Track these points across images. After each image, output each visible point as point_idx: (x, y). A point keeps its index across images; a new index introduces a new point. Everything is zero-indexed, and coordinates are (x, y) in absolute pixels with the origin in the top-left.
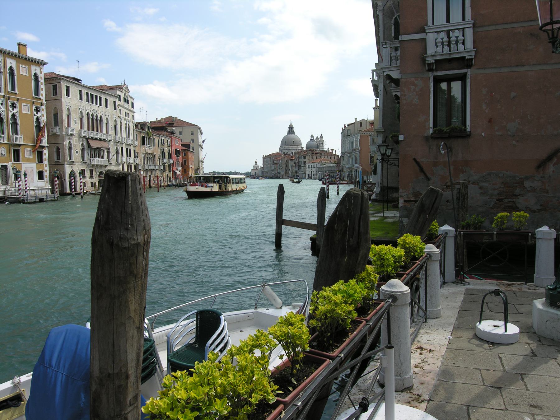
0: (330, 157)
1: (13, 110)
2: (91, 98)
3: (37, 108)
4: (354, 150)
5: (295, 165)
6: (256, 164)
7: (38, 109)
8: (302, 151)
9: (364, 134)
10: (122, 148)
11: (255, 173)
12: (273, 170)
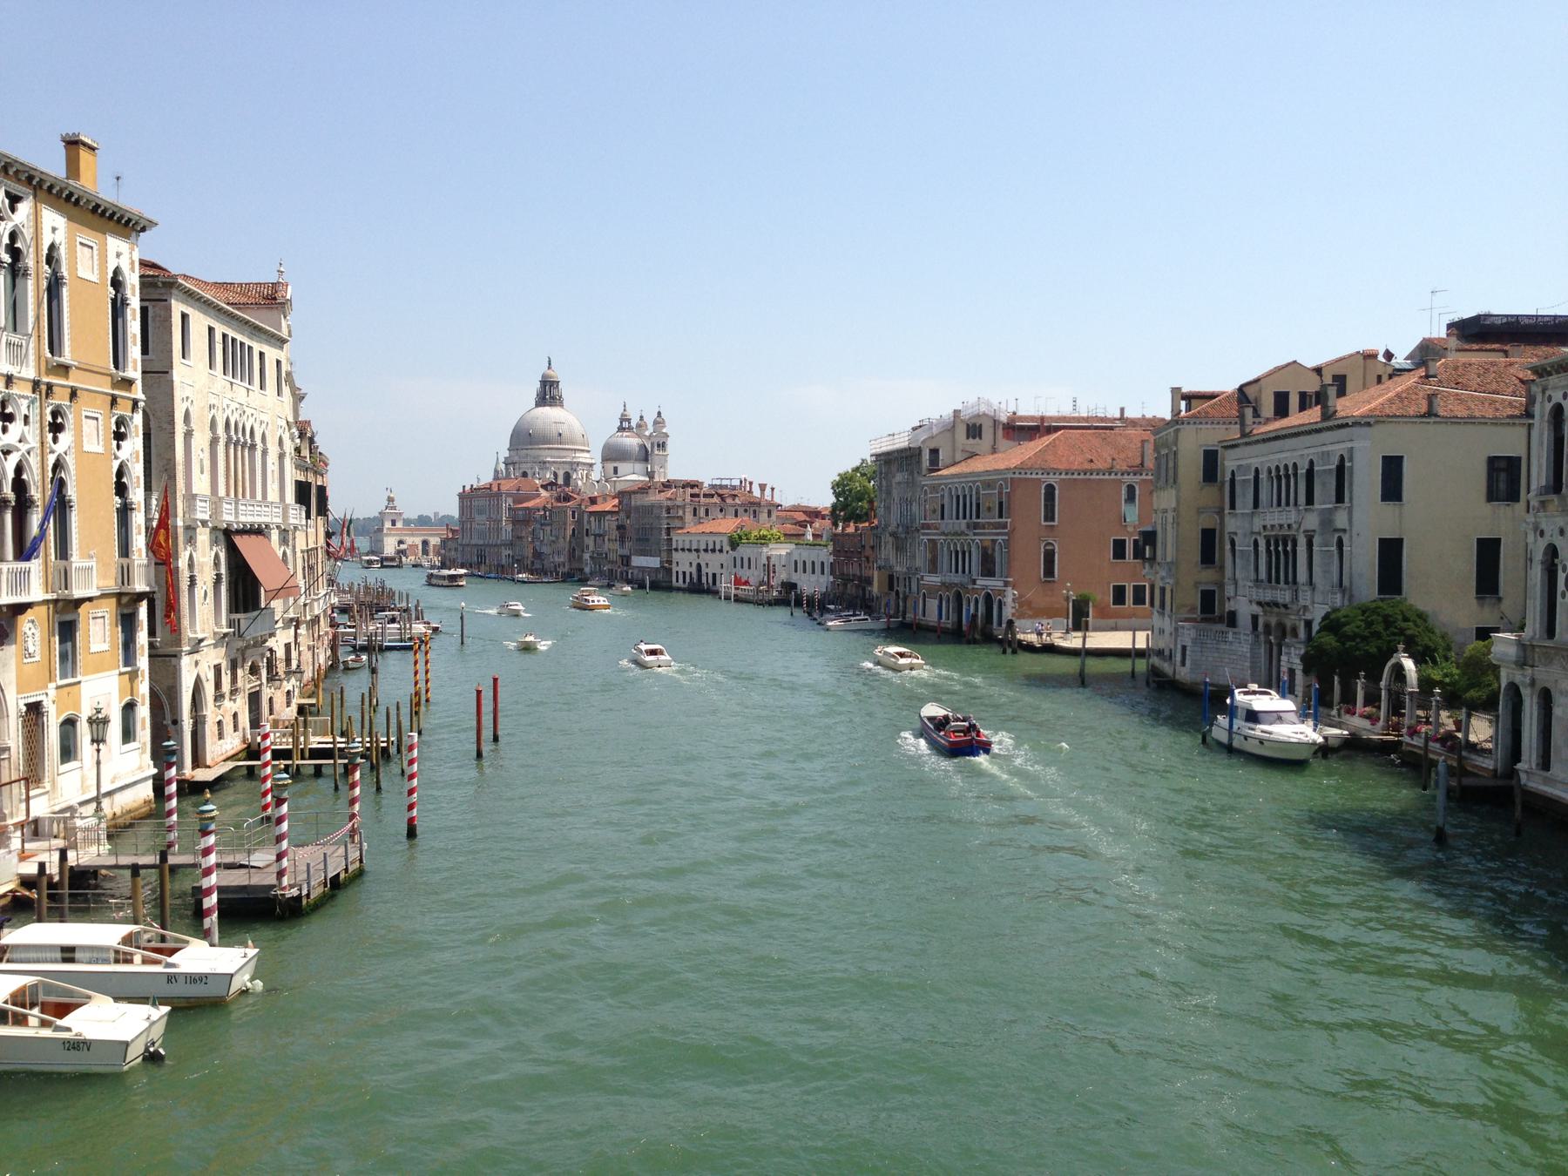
0: (755, 512)
1: (55, 440)
2: (235, 361)
3: (121, 422)
4: (976, 526)
7: (123, 430)
8: (649, 487)
9: (1023, 476)
11: (401, 542)
12: (511, 545)
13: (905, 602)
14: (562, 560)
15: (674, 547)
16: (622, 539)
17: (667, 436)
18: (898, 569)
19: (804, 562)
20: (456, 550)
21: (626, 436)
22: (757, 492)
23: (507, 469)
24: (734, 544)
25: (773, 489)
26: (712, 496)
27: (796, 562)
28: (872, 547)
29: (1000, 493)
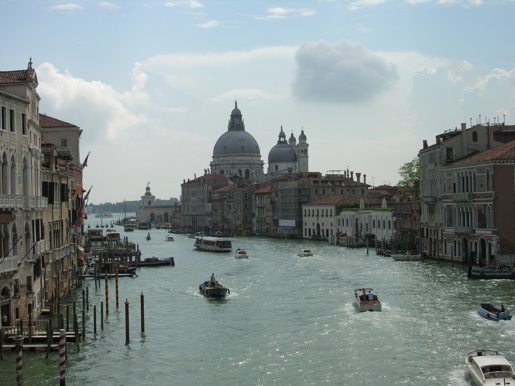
0: (354, 190)
4: (474, 196)
5: (274, 208)
6: (148, 194)
8: (289, 178)
10: (33, 221)
11: (152, 215)
12: (210, 215)
13: (435, 246)
14: (239, 223)
15: (304, 214)
16: (274, 209)
17: (308, 145)
18: (431, 225)
19: (379, 221)
20: (180, 218)
21: (283, 147)
22: (355, 179)
23: (212, 169)
24: (339, 209)
25: (365, 176)
26: (327, 182)
27: (374, 221)
28: (417, 211)
29: (488, 175)
